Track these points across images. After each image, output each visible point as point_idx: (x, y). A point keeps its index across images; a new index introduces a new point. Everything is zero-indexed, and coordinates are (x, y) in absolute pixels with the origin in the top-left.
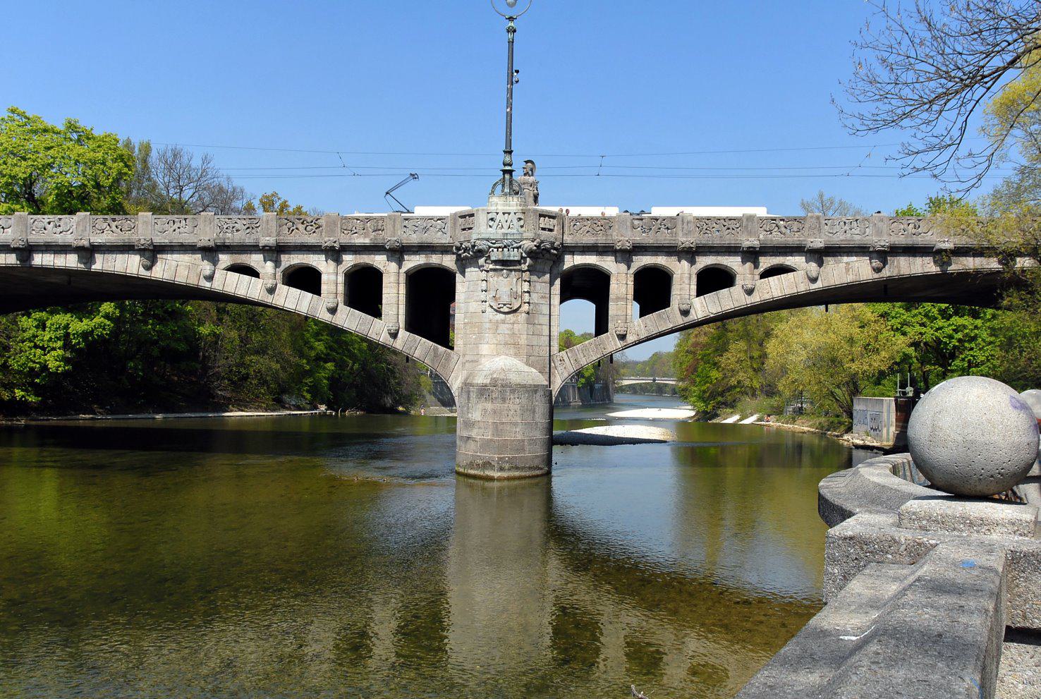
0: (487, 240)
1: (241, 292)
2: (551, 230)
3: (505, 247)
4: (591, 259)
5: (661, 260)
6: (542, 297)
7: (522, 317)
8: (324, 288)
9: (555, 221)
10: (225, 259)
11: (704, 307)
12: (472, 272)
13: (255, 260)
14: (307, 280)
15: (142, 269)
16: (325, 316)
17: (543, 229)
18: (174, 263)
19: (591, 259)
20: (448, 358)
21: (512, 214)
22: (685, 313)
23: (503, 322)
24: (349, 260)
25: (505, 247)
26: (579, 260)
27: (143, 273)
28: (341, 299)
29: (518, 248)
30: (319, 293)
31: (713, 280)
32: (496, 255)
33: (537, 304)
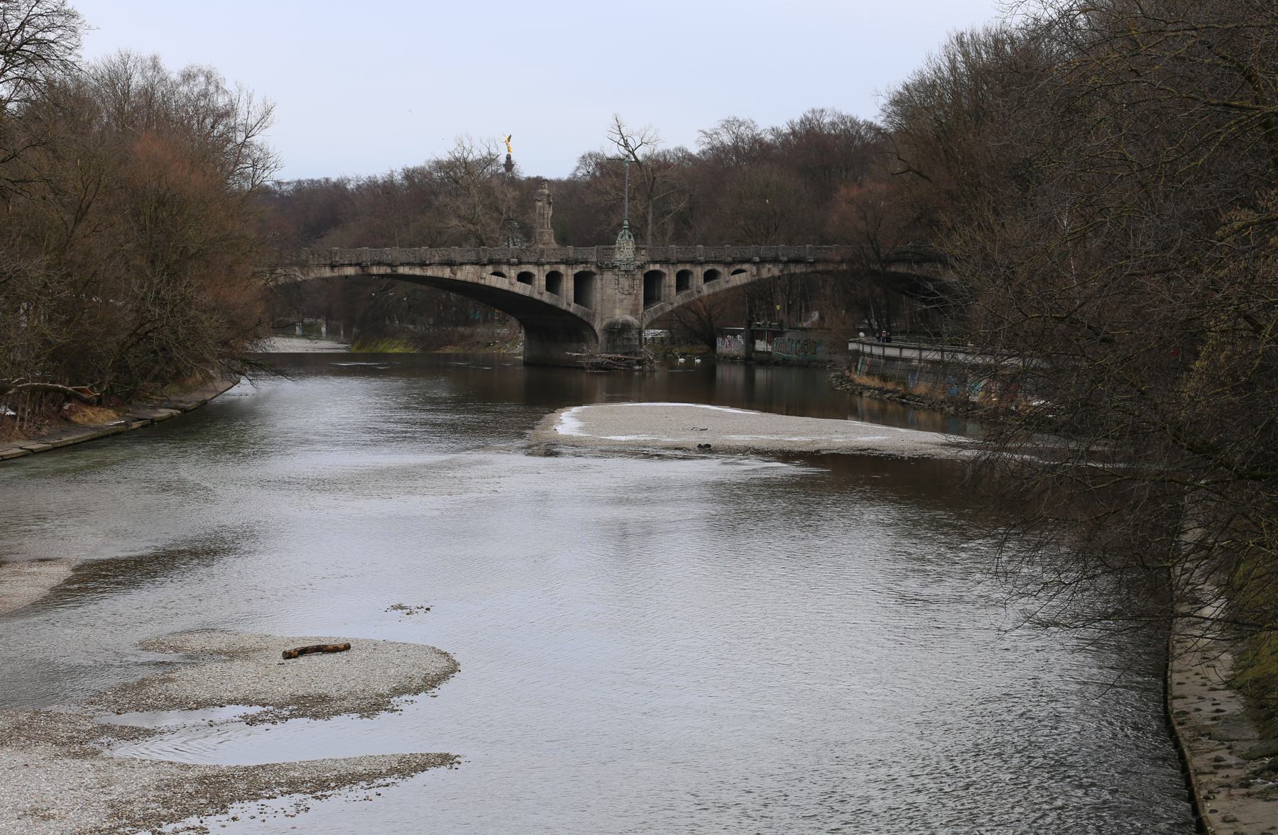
4: (657, 267)
5: (688, 267)
10: (490, 269)
11: (706, 290)
12: (608, 276)
13: (505, 269)
14: (525, 278)
16: (537, 297)
19: (657, 267)
24: (548, 268)
26: (652, 267)
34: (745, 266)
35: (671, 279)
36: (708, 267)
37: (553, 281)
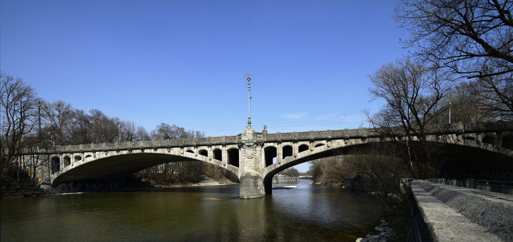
0: (245, 141)
1: (190, 157)
2: (260, 137)
3: (249, 142)
4: (272, 144)
5: (289, 144)
6: (259, 154)
7: (254, 160)
8: (208, 155)
9: (262, 135)
10: (186, 149)
12: (242, 149)
13: (192, 149)
14: (204, 153)
15: (168, 152)
17: (259, 137)
18: (175, 151)
19: (272, 144)
20: (238, 170)
21: (250, 134)
22: (295, 157)
23: (249, 161)
25: (249, 142)
26: (269, 145)
27: (168, 153)
28: (212, 157)
29: (252, 142)
30: (207, 156)
31: (303, 148)
32: (247, 144)
33: (258, 156)
34: (324, 142)
35: (280, 151)
36: (300, 143)
37: (218, 155)
